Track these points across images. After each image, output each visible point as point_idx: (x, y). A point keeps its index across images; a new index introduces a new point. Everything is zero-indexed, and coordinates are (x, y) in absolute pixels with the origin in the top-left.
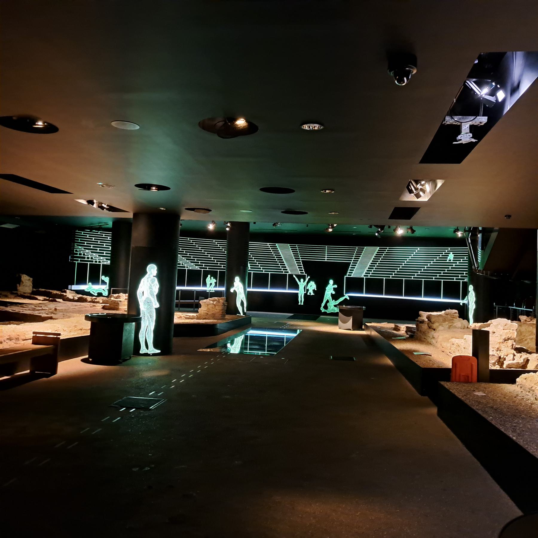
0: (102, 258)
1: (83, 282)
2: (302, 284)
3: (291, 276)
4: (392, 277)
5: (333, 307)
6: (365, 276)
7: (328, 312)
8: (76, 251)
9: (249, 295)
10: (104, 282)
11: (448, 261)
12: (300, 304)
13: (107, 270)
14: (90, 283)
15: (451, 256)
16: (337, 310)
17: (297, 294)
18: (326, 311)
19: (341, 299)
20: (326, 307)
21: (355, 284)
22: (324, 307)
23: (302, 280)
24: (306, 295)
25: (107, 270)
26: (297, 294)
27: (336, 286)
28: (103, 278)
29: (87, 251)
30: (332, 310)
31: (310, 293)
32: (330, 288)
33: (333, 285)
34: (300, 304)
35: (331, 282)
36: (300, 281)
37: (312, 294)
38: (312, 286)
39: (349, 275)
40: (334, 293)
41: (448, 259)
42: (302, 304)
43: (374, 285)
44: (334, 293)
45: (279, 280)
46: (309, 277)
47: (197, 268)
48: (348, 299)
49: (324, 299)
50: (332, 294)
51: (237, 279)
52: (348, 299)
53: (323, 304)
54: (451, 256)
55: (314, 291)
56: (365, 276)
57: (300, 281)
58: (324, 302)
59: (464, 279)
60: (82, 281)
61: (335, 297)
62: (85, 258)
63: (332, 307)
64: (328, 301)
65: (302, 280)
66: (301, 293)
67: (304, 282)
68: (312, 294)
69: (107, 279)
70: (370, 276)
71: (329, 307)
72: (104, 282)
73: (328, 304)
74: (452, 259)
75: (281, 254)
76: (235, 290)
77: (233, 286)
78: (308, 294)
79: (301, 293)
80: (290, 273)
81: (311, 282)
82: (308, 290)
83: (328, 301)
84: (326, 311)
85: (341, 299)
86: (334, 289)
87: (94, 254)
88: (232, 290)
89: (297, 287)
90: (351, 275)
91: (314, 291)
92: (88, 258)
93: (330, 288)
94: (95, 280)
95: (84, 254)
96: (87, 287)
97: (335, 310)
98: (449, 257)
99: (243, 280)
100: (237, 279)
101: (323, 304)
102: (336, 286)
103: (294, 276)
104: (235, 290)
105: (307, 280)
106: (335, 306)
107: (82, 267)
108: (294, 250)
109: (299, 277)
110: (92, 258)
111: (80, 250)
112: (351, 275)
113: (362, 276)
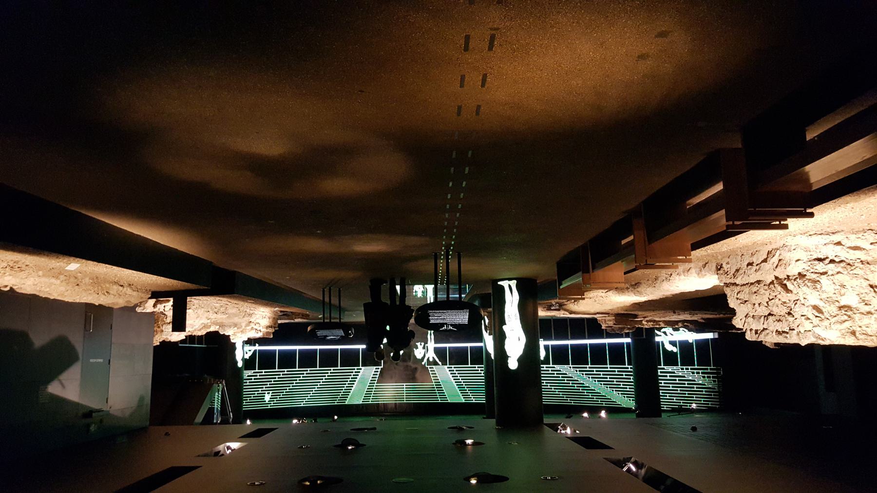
0: (680, 374)
1: (698, 342)
2: (431, 355)
3: (444, 363)
8: (714, 381)
9: (480, 339)
10: (673, 343)
13: (671, 359)
14: (691, 341)
15: (267, 398)
17: (435, 343)
23: (431, 360)
25: (671, 359)
26: (435, 343)
28: (675, 350)
29: (700, 382)
37: (418, 344)
45: (458, 358)
47: (557, 367)
54: (267, 398)
55: (417, 348)
60: (702, 344)
62: (703, 373)
65: (431, 360)
66: (432, 345)
68: (418, 344)
69: (669, 348)
72: (673, 343)
74: (266, 395)
75: (458, 390)
79: (432, 345)
80: (446, 367)
82: (424, 348)
87: (690, 378)
89: (437, 351)
91: (417, 348)
92: (698, 373)
94: (685, 346)
95: (704, 377)
96: (691, 337)
99: (488, 354)
105: (425, 360)
107: (704, 361)
109: (435, 363)
110: (693, 373)
111: (709, 383)
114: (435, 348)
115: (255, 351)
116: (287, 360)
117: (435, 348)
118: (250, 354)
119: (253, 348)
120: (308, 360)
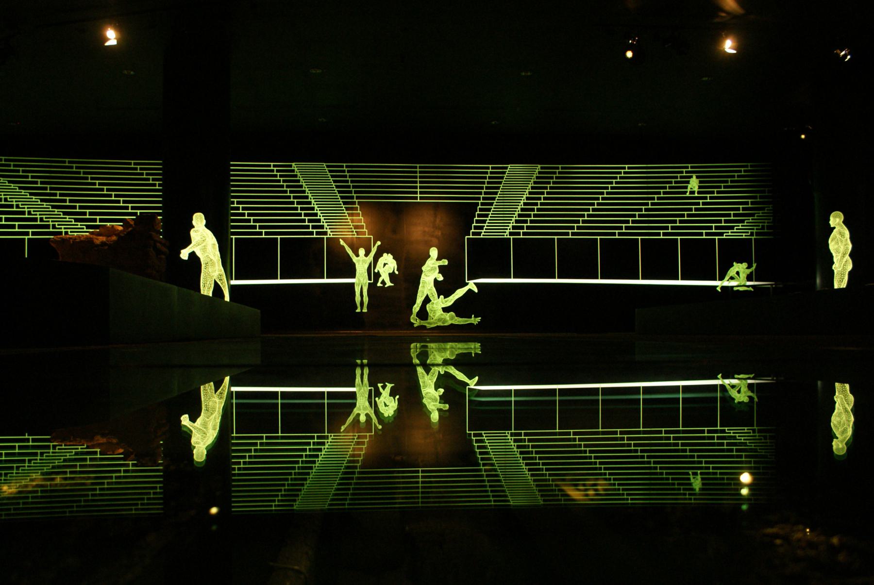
2: (361, 262)
4: (573, 234)
5: (439, 313)
6: (511, 234)
7: (428, 326)
11: (688, 195)
12: (358, 310)
15: (694, 184)
16: (451, 319)
18: (423, 323)
19: (460, 293)
20: (423, 314)
21: (490, 256)
22: (418, 314)
23: (362, 251)
24: (372, 287)
26: (353, 285)
27: (445, 262)
30: (439, 320)
31: (383, 282)
32: (431, 272)
33: (439, 259)
34: (358, 310)
35: (434, 252)
36: (357, 256)
38: (388, 265)
39: (474, 234)
40: (441, 278)
41: (689, 190)
42: (365, 310)
43: (532, 255)
44: (441, 278)
46: (379, 243)
48: (476, 290)
49: (419, 294)
50: (435, 280)
51: (199, 220)
52: (476, 290)
53: (416, 308)
54: (694, 184)
56: (511, 234)
57: (357, 256)
58: (420, 300)
59: (722, 234)
61: (443, 289)
63: (439, 309)
64: (427, 300)
65: (362, 251)
66: (361, 281)
67: (366, 255)
68: (389, 284)
70: (524, 234)
71: (431, 314)
73: (429, 307)
74: (696, 189)
76: (193, 255)
77: (187, 241)
78: (379, 284)
79: (361, 281)
80: (330, 235)
81: (385, 255)
82: (378, 275)
83: (427, 300)
84: (423, 323)
85: (460, 293)
86: (442, 269)
88: (184, 254)
89: (351, 271)
90: (479, 234)
91: (392, 276)
93: (431, 272)
97: (445, 321)
98: (690, 186)
100: (199, 220)
101: (416, 308)
102: (445, 262)
103: (342, 242)
104: (193, 255)
105: (374, 250)
106: (446, 310)
108: (339, 178)
112: (479, 234)
113: (506, 235)
114: (354, 276)
115: (722, 278)
116: (660, 259)
117: (354, 276)
118: (732, 272)
119: (726, 283)
120: (620, 257)
